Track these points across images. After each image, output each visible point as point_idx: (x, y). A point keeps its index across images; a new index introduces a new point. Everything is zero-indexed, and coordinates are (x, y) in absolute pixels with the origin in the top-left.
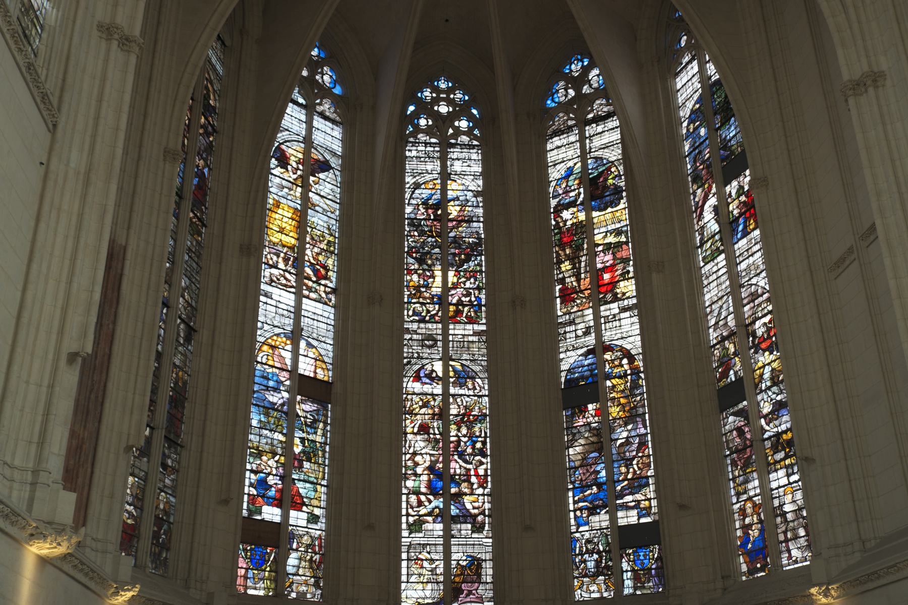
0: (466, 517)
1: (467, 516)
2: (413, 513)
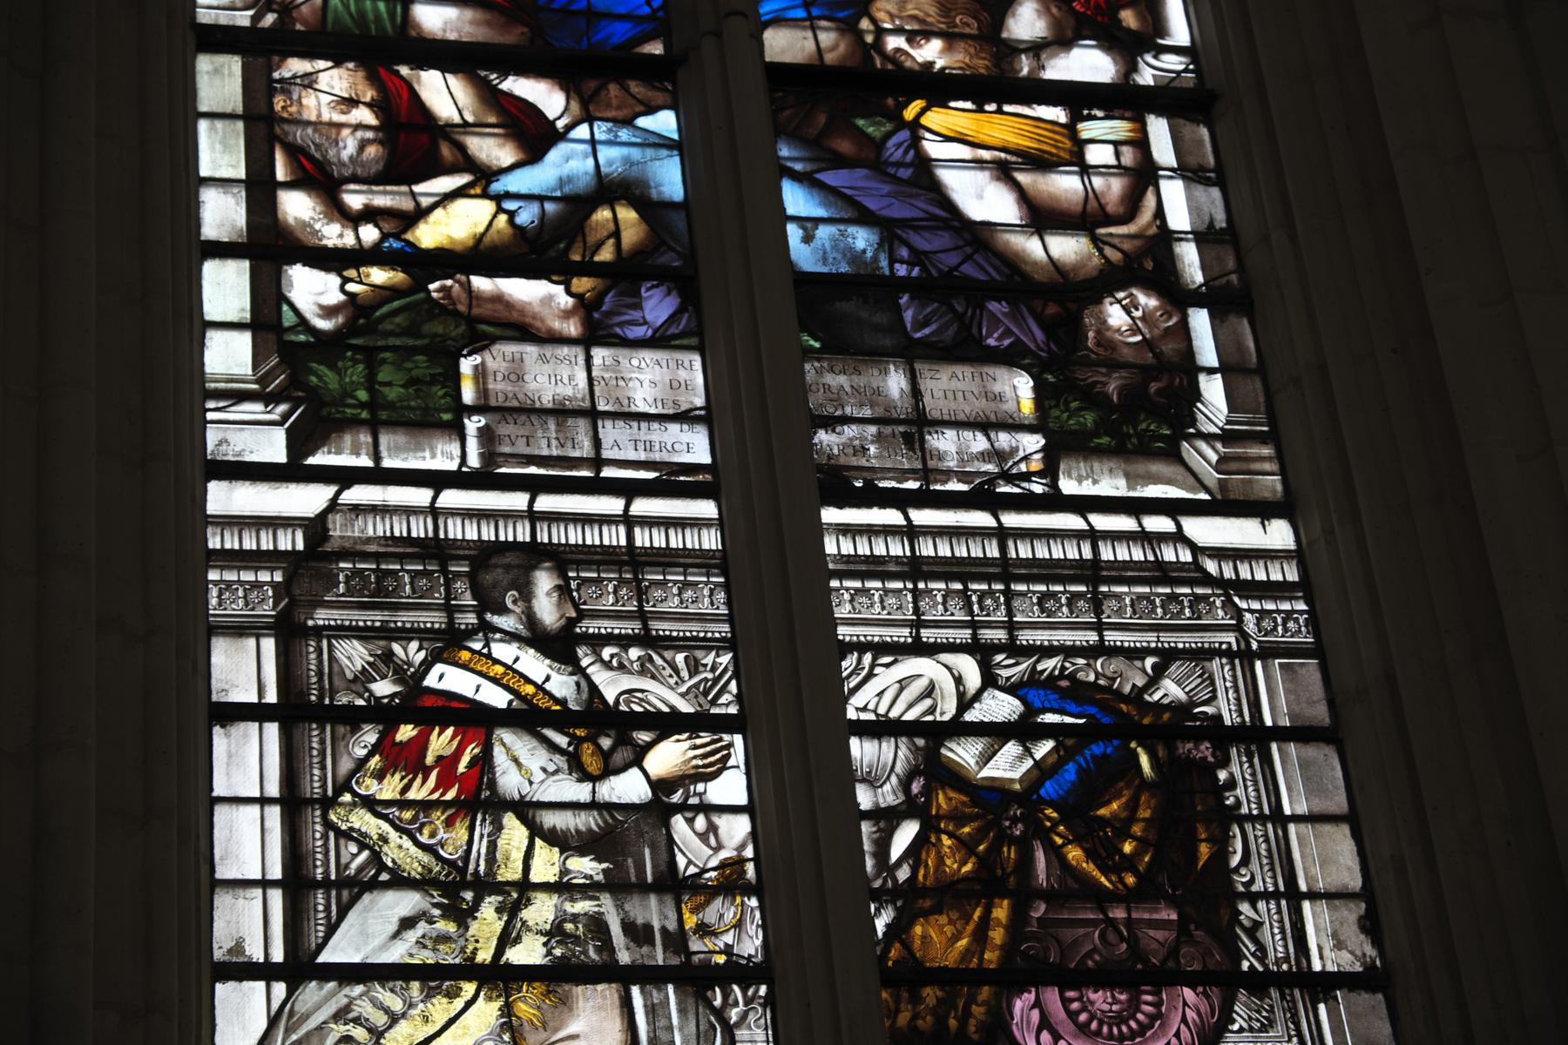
0: (955, 294)
1: (978, 293)
2: (334, 235)
